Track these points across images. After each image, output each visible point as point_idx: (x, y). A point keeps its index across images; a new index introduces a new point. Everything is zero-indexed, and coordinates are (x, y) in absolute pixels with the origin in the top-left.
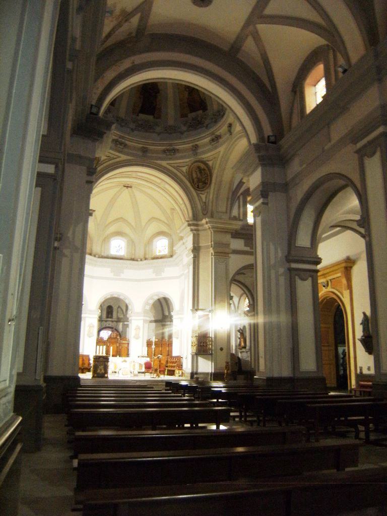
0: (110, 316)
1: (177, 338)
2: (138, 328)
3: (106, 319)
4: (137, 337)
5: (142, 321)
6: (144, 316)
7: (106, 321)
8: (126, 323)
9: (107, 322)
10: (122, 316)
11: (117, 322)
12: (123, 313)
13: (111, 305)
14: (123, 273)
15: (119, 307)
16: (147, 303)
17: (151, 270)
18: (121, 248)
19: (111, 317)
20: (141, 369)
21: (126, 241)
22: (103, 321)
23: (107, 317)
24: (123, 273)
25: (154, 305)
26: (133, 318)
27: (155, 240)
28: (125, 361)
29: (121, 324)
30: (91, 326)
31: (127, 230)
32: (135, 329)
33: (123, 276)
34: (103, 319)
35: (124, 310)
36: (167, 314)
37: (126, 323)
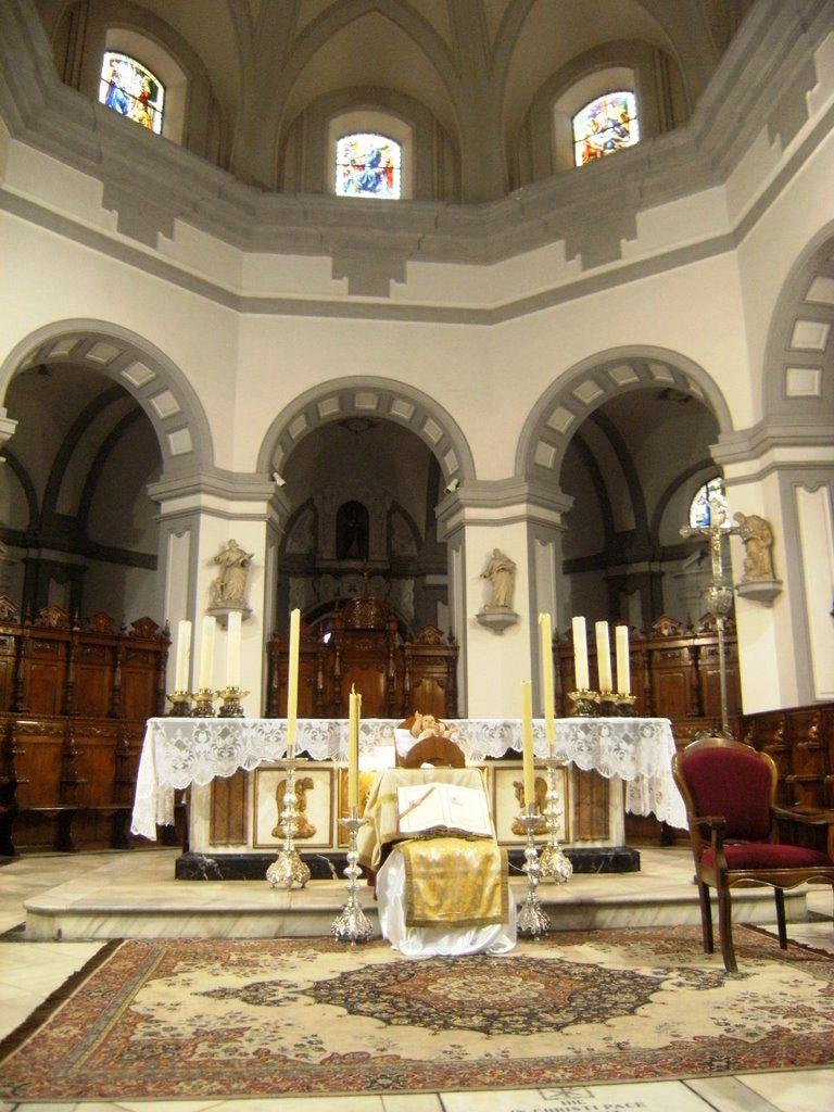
0: (354, 547)
1: (768, 598)
2: (500, 567)
3: (336, 565)
4: (499, 622)
5: (522, 528)
6: (528, 501)
7: (338, 574)
8: (431, 580)
9: (344, 579)
10: (411, 550)
11: (386, 574)
12: (415, 530)
13: (359, 498)
14: (401, 278)
15: (396, 508)
16: (539, 429)
17: (558, 246)
18: (388, 170)
19: (363, 554)
20: (605, 833)
21: (404, 129)
22: (319, 573)
23: (343, 554)
24: (401, 278)
25: (578, 442)
26: (470, 513)
27: (562, 104)
28: (441, 754)
29: (409, 586)
30: (233, 562)
31: (416, 72)
32: (487, 575)
33: (399, 294)
34: (319, 565)
35: (422, 527)
36: (631, 525)
37: (431, 580)
